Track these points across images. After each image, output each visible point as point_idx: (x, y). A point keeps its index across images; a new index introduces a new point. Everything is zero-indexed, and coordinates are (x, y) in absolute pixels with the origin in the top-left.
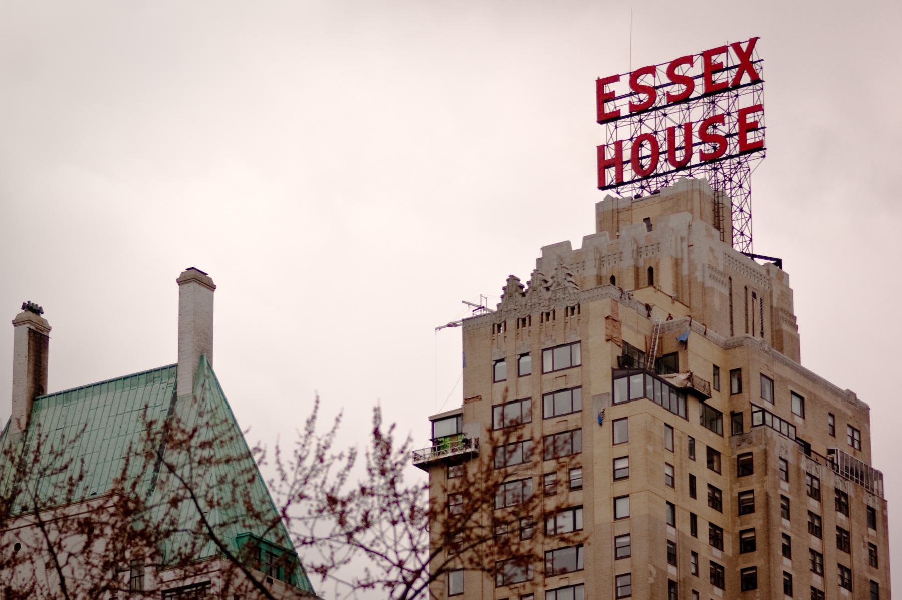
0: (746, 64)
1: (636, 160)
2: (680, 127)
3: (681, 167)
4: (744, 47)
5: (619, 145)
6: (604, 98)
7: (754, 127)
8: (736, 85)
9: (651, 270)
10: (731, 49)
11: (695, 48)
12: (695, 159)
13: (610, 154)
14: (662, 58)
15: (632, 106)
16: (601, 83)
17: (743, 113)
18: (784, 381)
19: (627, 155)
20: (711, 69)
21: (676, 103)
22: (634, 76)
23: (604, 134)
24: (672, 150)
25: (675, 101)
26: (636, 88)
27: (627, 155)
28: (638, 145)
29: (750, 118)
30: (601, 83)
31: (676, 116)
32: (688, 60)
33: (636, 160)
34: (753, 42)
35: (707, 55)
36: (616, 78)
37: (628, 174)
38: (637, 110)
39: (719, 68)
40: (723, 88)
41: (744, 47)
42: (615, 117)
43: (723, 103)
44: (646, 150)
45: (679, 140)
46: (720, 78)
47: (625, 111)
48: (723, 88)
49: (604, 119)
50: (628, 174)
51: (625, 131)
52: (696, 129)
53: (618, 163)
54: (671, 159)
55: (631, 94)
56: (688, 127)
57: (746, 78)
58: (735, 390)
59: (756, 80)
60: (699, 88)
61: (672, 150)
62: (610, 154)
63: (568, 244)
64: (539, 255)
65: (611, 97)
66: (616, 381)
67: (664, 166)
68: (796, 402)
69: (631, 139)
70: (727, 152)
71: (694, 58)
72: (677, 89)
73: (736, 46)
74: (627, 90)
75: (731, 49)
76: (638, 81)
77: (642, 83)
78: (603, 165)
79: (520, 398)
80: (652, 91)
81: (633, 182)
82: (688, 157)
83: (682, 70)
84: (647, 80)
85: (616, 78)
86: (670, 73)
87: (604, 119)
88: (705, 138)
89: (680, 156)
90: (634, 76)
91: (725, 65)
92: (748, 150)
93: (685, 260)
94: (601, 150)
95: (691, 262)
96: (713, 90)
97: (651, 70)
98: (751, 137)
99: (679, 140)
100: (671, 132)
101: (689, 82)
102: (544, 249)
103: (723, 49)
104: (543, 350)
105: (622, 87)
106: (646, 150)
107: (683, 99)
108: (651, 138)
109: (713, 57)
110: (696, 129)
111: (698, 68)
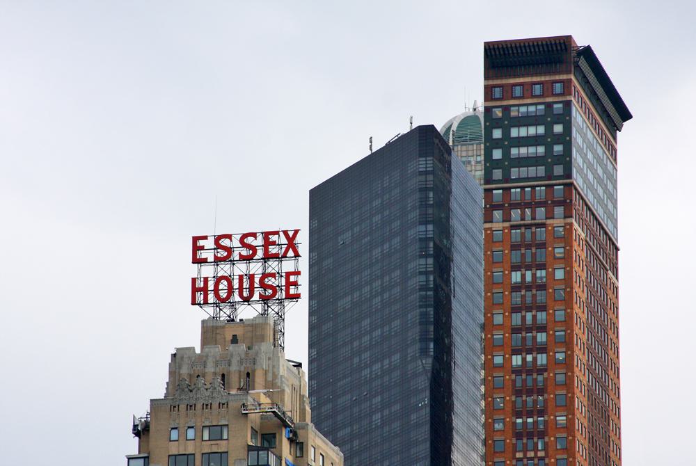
1: (216, 290)
2: (246, 275)
3: (247, 300)
4: (291, 234)
5: (206, 280)
6: (196, 249)
8: (285, 256)
9: (248, 374)
10: (281, 234)
11: (259, 228)
12: (256, 297)
14: (237, 229)
15: (216, 257)
16: (195, 239)
17: (288, 274)
18: (319, 447)
19: (211, 286)
20: (267, 243)
21: (244, 260)
22: (218, 239)
23: (193, 270)
25: (242, 258)
26: (218, 246)
27: (211, 286)
28: (218, 280)
29: (292, 278)
30: (195, 239)
31: (241, 268)
32: (254, 235)
33: (216, 290)
34: (296, 232)
35: (266, 235)
36: (205, 238)
37: (211, 298)
38: (218, 260)
39: (274, 243)
40: (276, 256)
41: (291, 234)
42: (205, 261)
43: (273, 266)
44: (223, 285)
45: (246, 284)
46: (273, 250)
47: (211, 259)
48: (276, 256)
49: (197, 261)
50: (211, 298)
51: (208, 271)
52: (257, 280)
53: (205, 290)
54: (241, 295)
55: (214, 249)
56: (251, 277)
57: (291, 253)
58: (298, 455)
60: (260, 254)
61: (241, 289)
63: (193, 349)
64: (174, 352)
65: (202, 248)
66: (250, 452)
68: (321, 457)
69: (214, 277)
70: (277, 297)
71: (258, 235)
72: (245, 252)
73: (286, 233)
74: (213, 246)
75: (281, 234)
76: (220, 242)
77: (222, 244)
78: (195, 290)
79: (187, 453)
80: (229, 250)
81: (214, 303)
82: (252, 294)
83: (250, 240)
84: (225, 242)
85: (205, 238)
86: (242, 241)
88: (263, 286)
89: (245, 294)
90: (218, 239)
91: (277, 242)
92: (291, 297)
93: (271, 371)
94: (194, 280)
95: (274, 373)
96: (267, 257)
97: (229, 237)
98: (292, 291)
99: (246, 284)
100: (241, 277)
101: (254, 249)
102: (178, 349)
103: (277, 233)
104: (203, 427)
105: (209, 244)
106: (223, 285)
107: (248, 259)
108: (229, 279)
109: (270, 236)
110: (257, 280)
111: (259, 241)
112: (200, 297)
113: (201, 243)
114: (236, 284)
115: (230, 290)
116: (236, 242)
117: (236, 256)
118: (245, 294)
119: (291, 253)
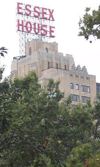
0: (51, 16)
1: (26, 26)
6: (19, 8)
7: (53, 32)
11: (41, 6)
13: (20, 23)
14: (34, 4)
16: (18, 4)
19: (24, 25)
24: (35, 29)
27: (24, 25)
30: (18, 4)
34: (53, 11)
35: (43, 9)
41: (51, 11)
42: (21, 14)
45: (37, 27)
53: (22, 25)
54: (35, 31)
57: (51, 19)
59: (53, 20)
62: (20, 23)
65: (21, 8)
67: (33, 31)
78: (19, 25)
85: (22, 4)
87: (19, 13)
97: (30, 6)
99: (37, 27)
105: (23, 7)
112: (21, 27)
113: (20, 6)
114: (33, 27)
115: (31, 28)
116: (32, 9)
117: (32, 15)
118: (37, 31)
119: (51, 19)
